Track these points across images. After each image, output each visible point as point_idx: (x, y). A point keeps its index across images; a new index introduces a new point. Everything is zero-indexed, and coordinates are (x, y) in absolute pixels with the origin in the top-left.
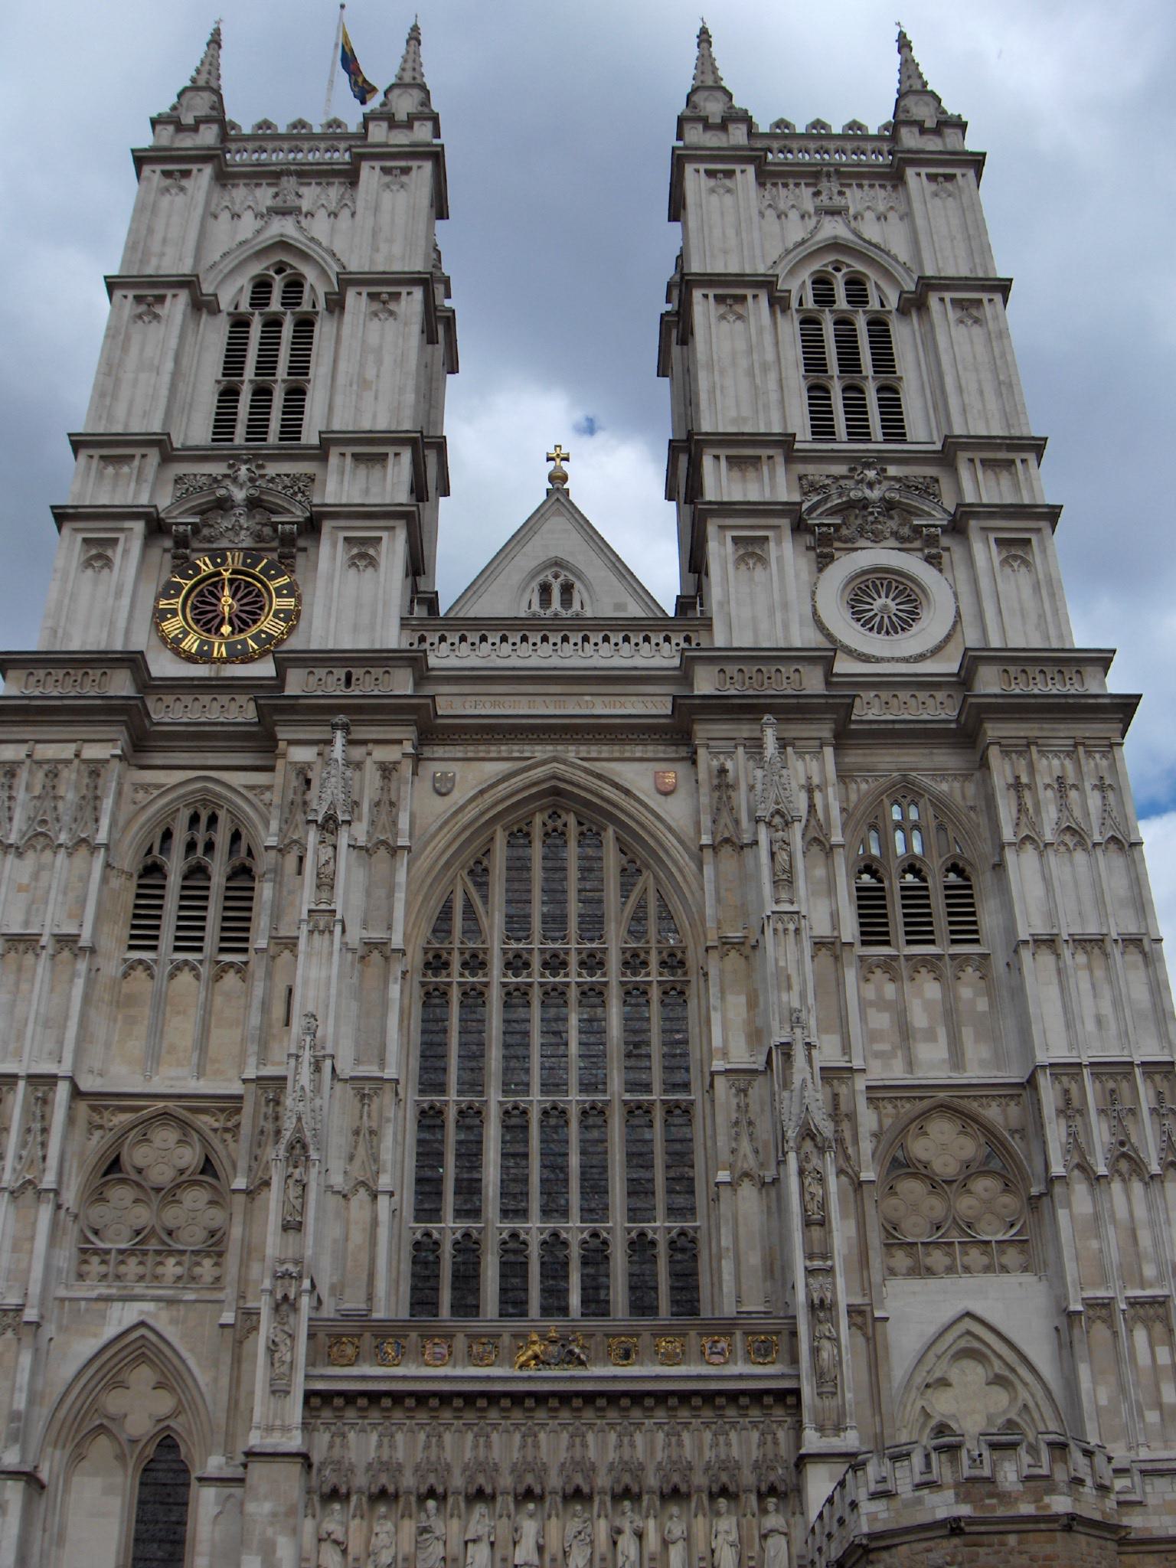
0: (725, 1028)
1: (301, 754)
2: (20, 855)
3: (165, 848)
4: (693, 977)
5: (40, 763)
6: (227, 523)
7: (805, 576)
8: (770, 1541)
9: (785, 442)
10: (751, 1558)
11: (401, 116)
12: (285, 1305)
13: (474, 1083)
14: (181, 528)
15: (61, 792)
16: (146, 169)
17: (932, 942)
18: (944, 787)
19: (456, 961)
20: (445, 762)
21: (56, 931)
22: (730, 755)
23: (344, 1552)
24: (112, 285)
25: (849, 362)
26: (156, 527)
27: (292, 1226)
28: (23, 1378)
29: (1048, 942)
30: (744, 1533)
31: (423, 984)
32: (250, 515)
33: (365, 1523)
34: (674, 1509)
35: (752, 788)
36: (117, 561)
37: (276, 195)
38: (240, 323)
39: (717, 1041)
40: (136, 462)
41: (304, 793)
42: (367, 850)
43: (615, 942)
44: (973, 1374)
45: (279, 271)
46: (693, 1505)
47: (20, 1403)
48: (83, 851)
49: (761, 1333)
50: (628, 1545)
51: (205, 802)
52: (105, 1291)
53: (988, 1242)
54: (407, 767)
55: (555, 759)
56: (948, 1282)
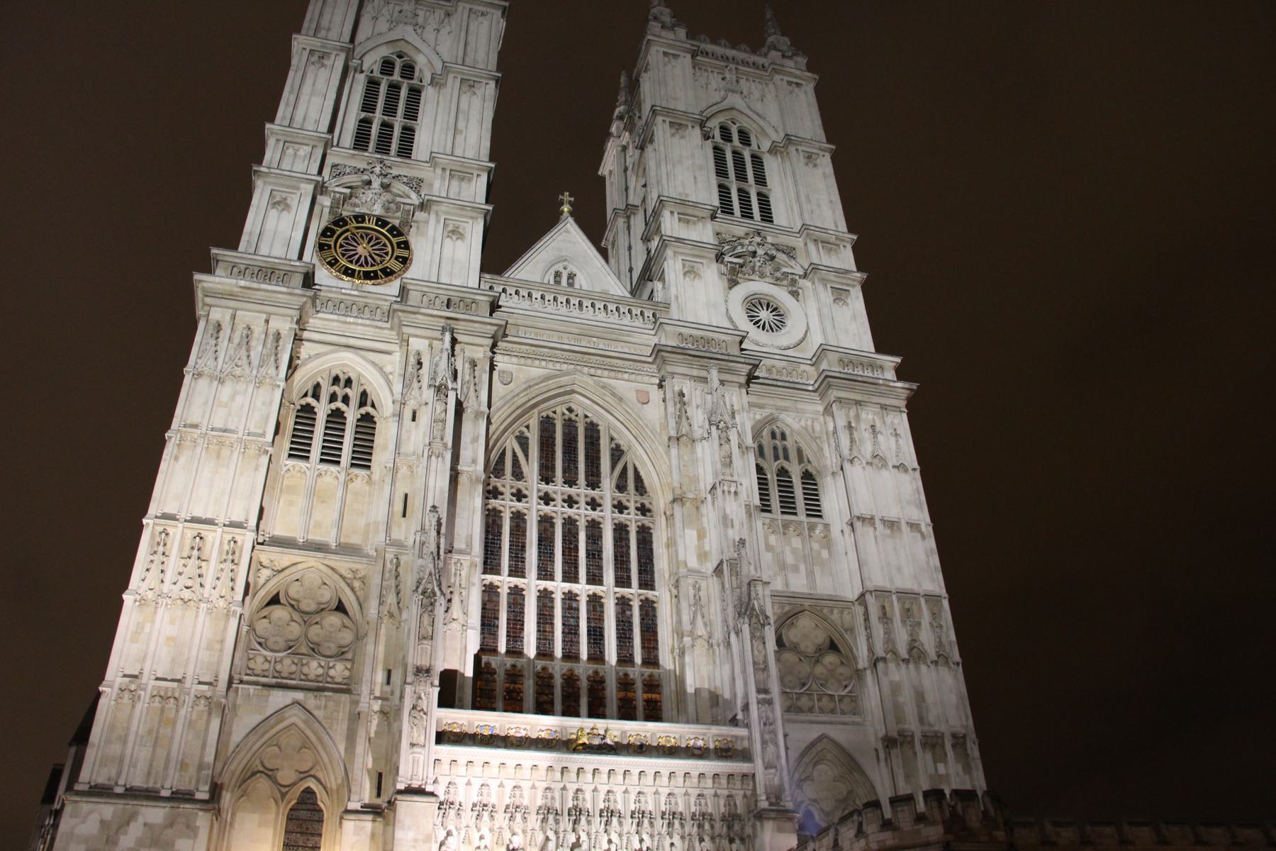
2: (221, 381)
3: (316, 396)
4: (657, 519)
14: (338, 195)
15: (253, 343)
17: (795, 514)
18: (803, 423)
29: (870, 520)
36: (294, 204)
37: (400, 12)
38: (373, 84)
39: (681, 557)
41: (419, 369)
43: (607, 491)
45: (400, 57)
53: (834, 696)
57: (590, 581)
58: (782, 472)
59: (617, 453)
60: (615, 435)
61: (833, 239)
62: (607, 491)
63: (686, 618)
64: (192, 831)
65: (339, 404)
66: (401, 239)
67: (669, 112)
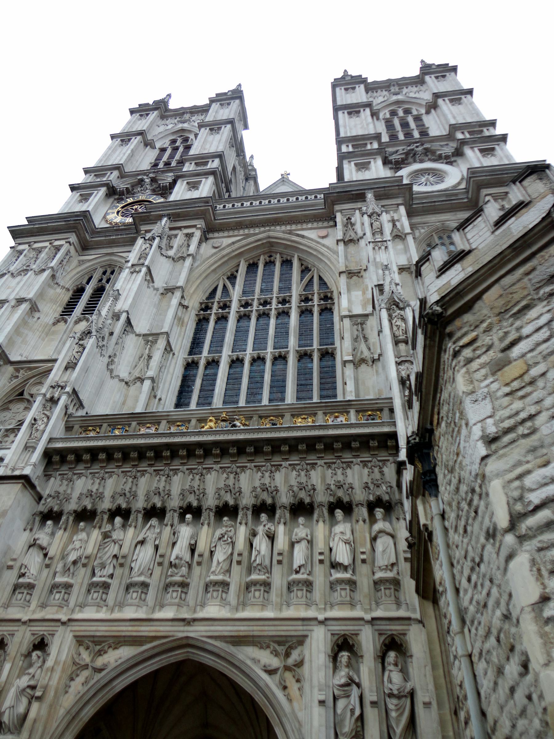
0: (350, 301)
5: (33, 249)
6: (139, 189)
8: (379, 541)
9: (378, 137)
10: (363, 553)
16: (134, 115)
19: (215, 306)
21: (18, 297)
22: (353, 215)
23: (45, 555)
24: (113, 137)
30: (357, 535)
31: (197, 315)
32: (151, 185)
33: (66, 534)
34: (301, 520)
42: (173, 259)
46: (315, 516)
49: (368, 411)
51: (110, 265)
54: (198, 234)
55: (269, 231)
60: (304, 263)
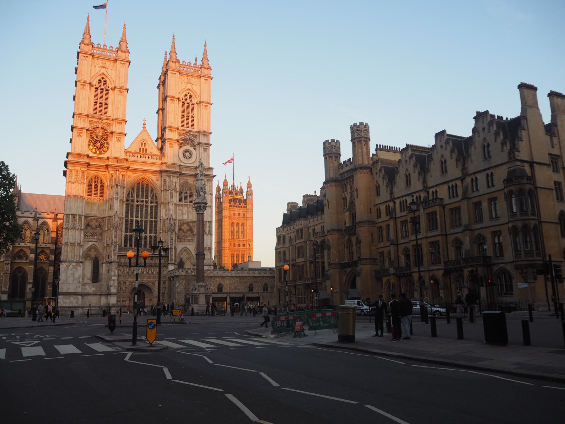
0: (163, 213)
1: (112, 172)
2: (73, 183)
5: (75, 170)
7: (178, 149)
11: (123, 50)
12: (115, 246)
13: (132, 216)
19: (130, 200)
20: (130, 173)
23: (121, 271)
25: (188, 112)
26: (87, 130)
27: (116, 237)
28: (81, 252)
35: (168, 182)
36: (83, 137)
38: (97, 88)
39: (162, 215)
40: (84, 118)
43: (149, 199)
44: (185, 253)
45: (103, 78)
47: (81, 255)
48: (82, 183)
50: (150, 271)
52: (88, 240)
55: (144, 175)
56: (184, 243)
57: (145, 218)
58: (186, 193)
59: (152, 191)
61: (206, 134)
62: (149, 199)
63: (161, 227)
64: (80, 266)
65: (96, 183)
66: (106, 142)
67: (170, 97)
